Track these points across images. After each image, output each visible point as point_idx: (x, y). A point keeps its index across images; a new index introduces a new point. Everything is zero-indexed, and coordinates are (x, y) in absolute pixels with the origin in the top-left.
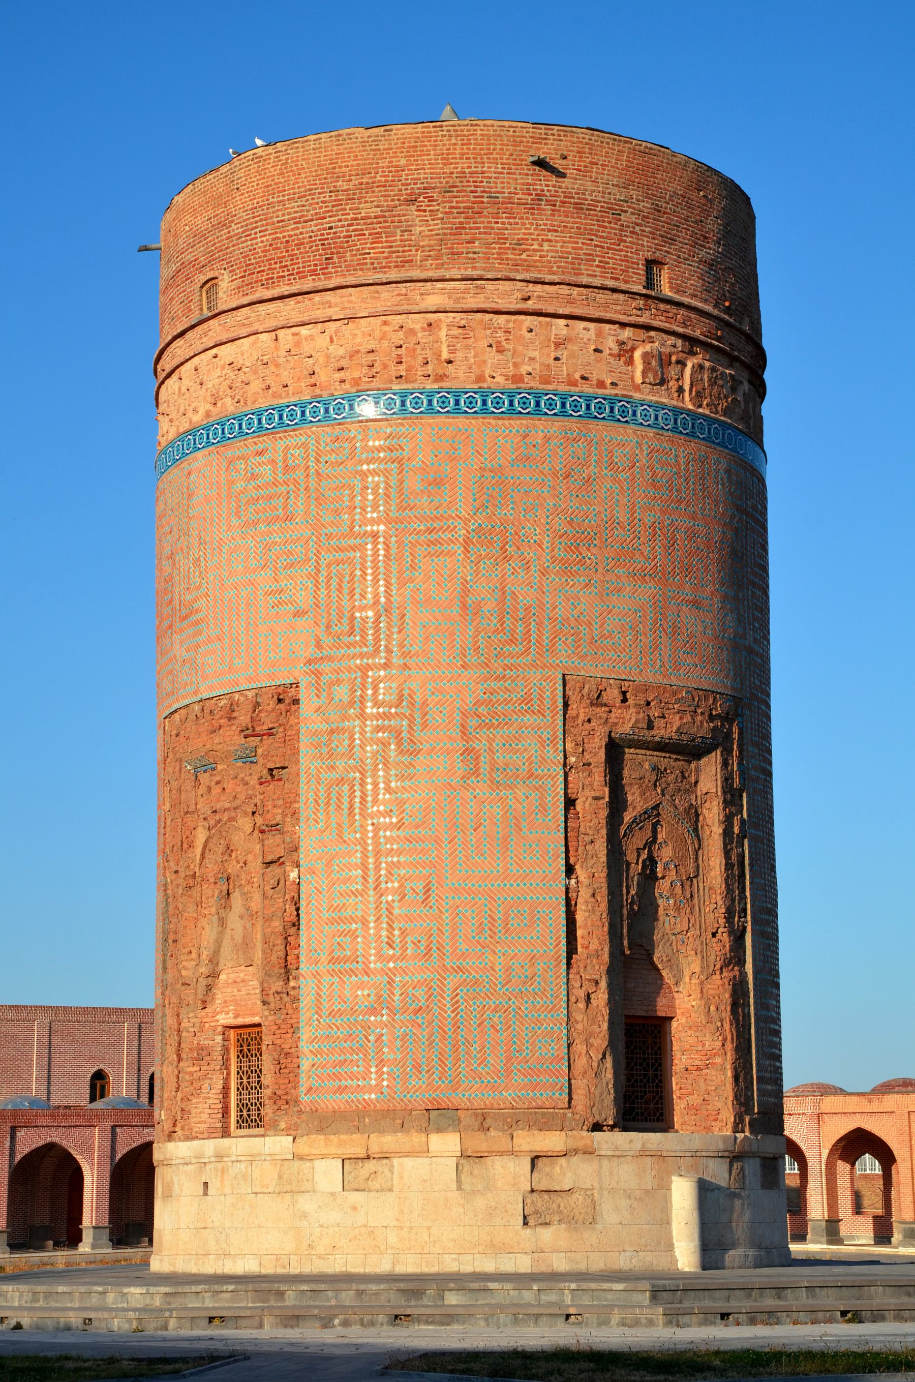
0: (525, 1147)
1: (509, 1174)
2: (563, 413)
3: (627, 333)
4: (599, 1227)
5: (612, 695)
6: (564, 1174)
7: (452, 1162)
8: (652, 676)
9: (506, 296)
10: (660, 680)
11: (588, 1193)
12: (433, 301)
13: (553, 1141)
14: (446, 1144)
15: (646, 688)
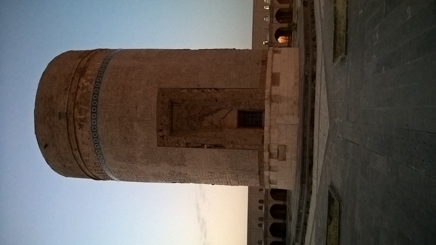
0: (268, 160)
1: (274, 162)
2: (98, 143)
3: (76, 125)
4: (287, 145)
5: (160, 134)
6: (274, 151)
7: (271, 172)
8: (155, 124)
9: (77, 154)
10: (155, 121)
11: (278, 146)
12: (83, 164)
13: (266, 154)
14: (266, 173)
15: (157, 124)
